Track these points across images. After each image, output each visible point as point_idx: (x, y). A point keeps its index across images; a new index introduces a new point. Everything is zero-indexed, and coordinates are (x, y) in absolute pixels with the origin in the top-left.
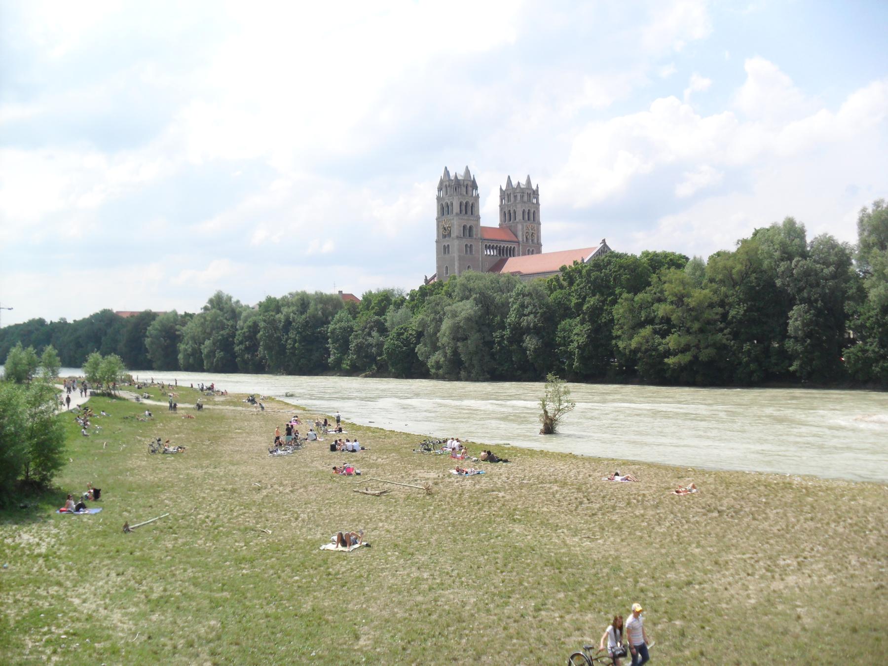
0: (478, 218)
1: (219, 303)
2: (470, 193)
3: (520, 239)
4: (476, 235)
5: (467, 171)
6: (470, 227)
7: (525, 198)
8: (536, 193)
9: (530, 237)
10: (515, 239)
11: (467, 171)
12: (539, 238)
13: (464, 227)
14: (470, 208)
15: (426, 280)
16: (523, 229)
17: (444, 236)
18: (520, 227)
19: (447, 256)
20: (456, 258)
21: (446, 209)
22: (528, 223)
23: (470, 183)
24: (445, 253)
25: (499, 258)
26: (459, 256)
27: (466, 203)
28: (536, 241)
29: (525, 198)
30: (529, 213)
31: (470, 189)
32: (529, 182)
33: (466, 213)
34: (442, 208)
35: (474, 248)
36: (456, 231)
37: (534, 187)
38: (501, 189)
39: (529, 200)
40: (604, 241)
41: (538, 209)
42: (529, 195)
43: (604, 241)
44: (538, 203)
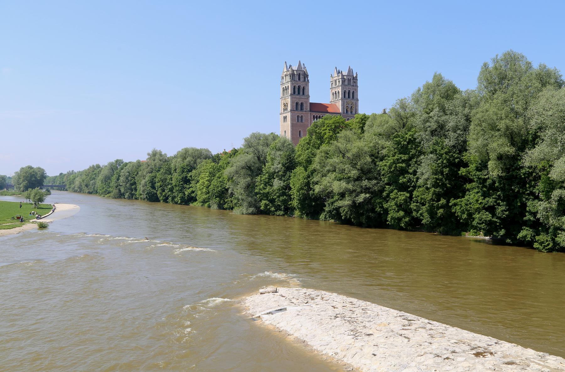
0: (308, 96)
4: (306, 109)
6: (302, 104)
7: (346, 83)
8: (355, 79)
13: (297, 103)
19: (285, 124)
22: (348, 100)
23: (301, 73)
24: (284, 121)
27: (299, 87)
29: (346, 83)
33: (299, 93)
34: (284, 90)
35: (304, 118)
37: (355, 76)
41: (356, 90)
42: (349, 80)
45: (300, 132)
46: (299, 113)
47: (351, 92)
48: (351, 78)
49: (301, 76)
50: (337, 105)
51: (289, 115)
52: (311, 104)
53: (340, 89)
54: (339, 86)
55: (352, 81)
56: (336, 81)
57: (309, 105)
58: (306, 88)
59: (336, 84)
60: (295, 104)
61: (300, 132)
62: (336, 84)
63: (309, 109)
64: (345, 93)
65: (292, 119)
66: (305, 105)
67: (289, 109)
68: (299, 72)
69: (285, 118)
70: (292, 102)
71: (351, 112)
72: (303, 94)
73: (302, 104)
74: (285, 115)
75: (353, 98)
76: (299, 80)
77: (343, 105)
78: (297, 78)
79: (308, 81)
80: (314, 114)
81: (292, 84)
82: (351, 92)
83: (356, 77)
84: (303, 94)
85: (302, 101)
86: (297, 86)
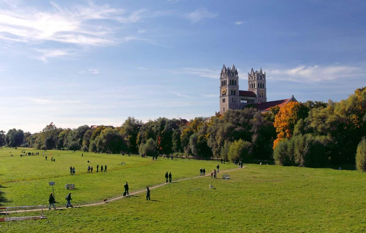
1: (130, 122)
2: (234, 76)
4: (237, 94)
5: (234, 67)
8: (264, 76)
11: (234, 67)
12: (265, 95)
13: (232, 91)
14: (234, 83)
15: (216, 113)
17: (223, 95)
19: (224, 103)
23: (234, 72)
24: (223, 102)
25: (247, 104)
29: (259, 78)
31: (235, 74)
32: (261, 71)
37: (264, 74)
38: (249, 74)
39: (261, 79)
41: (265, 83)
42: (261, 77)
43: (293, 96)
44: (265, 80)
46: (232, 97)
47: (262, 84)
48: (262, 75)
50: (254, 91)
51: (227, 98)
52: (240, 91)
53: (256, 82)
54: (255, 80)
55: (262, 77)
56: (252, 77)
59: (252, 79)
60: (231, 91)
62: (252, 79)
63: (238, 94)
64: (259, 84)
65: (229, 101)
66: (236, 92)
67: (227, 94)
68: (232, 72)
69: (224, 100)
70: (229, 90)
73: (235, 91)
74: (224, 98)
75: (263, 88)
76: (233, 76)
77: (258, 92)
78: (232, 74)
79: (238, 77)
80: (241, 97)
81: (229, 79)
82: (262, 84)
83: (265, 74)
85: (235, 89)
86: (232, 80)
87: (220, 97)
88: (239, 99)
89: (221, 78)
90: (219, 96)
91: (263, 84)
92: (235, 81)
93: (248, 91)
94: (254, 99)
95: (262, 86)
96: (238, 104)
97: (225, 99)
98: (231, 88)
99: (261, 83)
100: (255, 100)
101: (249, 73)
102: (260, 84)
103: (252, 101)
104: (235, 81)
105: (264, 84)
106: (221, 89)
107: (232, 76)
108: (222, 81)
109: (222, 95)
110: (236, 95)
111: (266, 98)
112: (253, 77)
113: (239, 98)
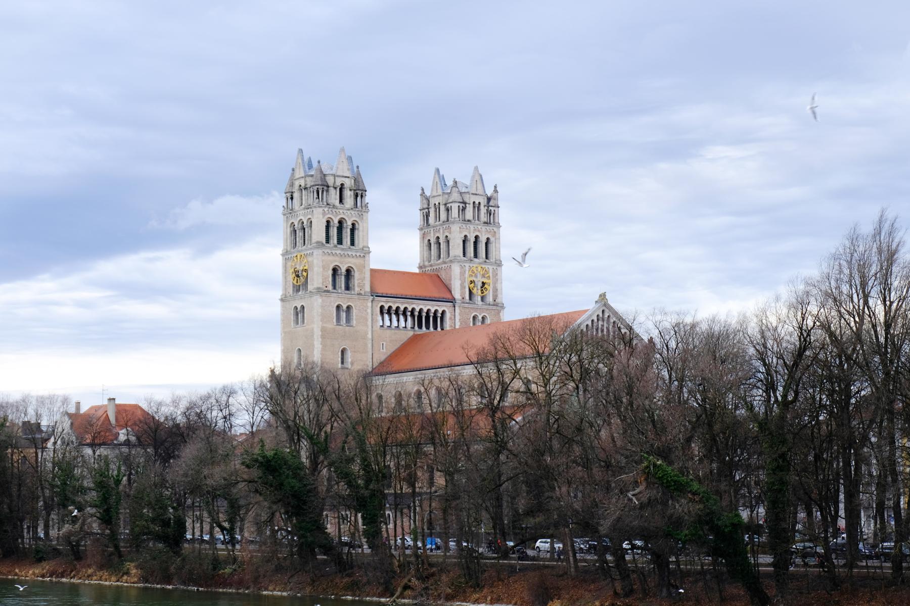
0: (366, 252)
3: (457, 295)
4: (361, 287)
6: (348, 271)
7: (469, 213)
9: (477, 291)
10: (448, 296)
13: (335, 270)
16: (462, 274)
17: (297, 289)
18: (456, 269)
19: (300, 329)
20: (317, 333)
21: (300, 234)
23: (348, 183)
25: (411, 333)
26: (323, 330)
28: (490, 299)
30: (476, 243)
33: (340, 241)
35: (354, 312)
36: (319, 277)
40: (603, 296)
42: (477, 207)
45: (343, 352)
47: (483, 240)
48: (483, 201)
49: (348, 194)
55: (483, 210)
56: (437, 208)
57: (368, 275)
58: (360, 227)
59: (437, 217)
60: (330, 272)
61: (343, 352)
62: (437, 217)
63: (367, 288)
69: (299, 312)
71: (483, 299)
72: (353, 243)
76: (341, 201)
82: (483, 240)
84: (353, 243)
86: (336, 221)
87: (282, 300)
88: (369, 311)
89: (289, 211)
90: (279, 293)
91: (488, 239)
92: (351, 227)
93: (417, 271)
94: (443, 312)
95: (480, 248)
96: (367, 334)
97: (303, 307)
98: (331, 258)
99: (477, 237)
100: (448, 315)
101: (423, 190)
102: (473, 240)
103: (435, 318)
104: (353, 225)
105: (492, 239)
106: (289, 264)
107: (338, 201)
108: (293, 224)
109: (291, 290)
110: (357, 289)
111: (498, 306)
112: (442, 208)
113: (370, 304)
